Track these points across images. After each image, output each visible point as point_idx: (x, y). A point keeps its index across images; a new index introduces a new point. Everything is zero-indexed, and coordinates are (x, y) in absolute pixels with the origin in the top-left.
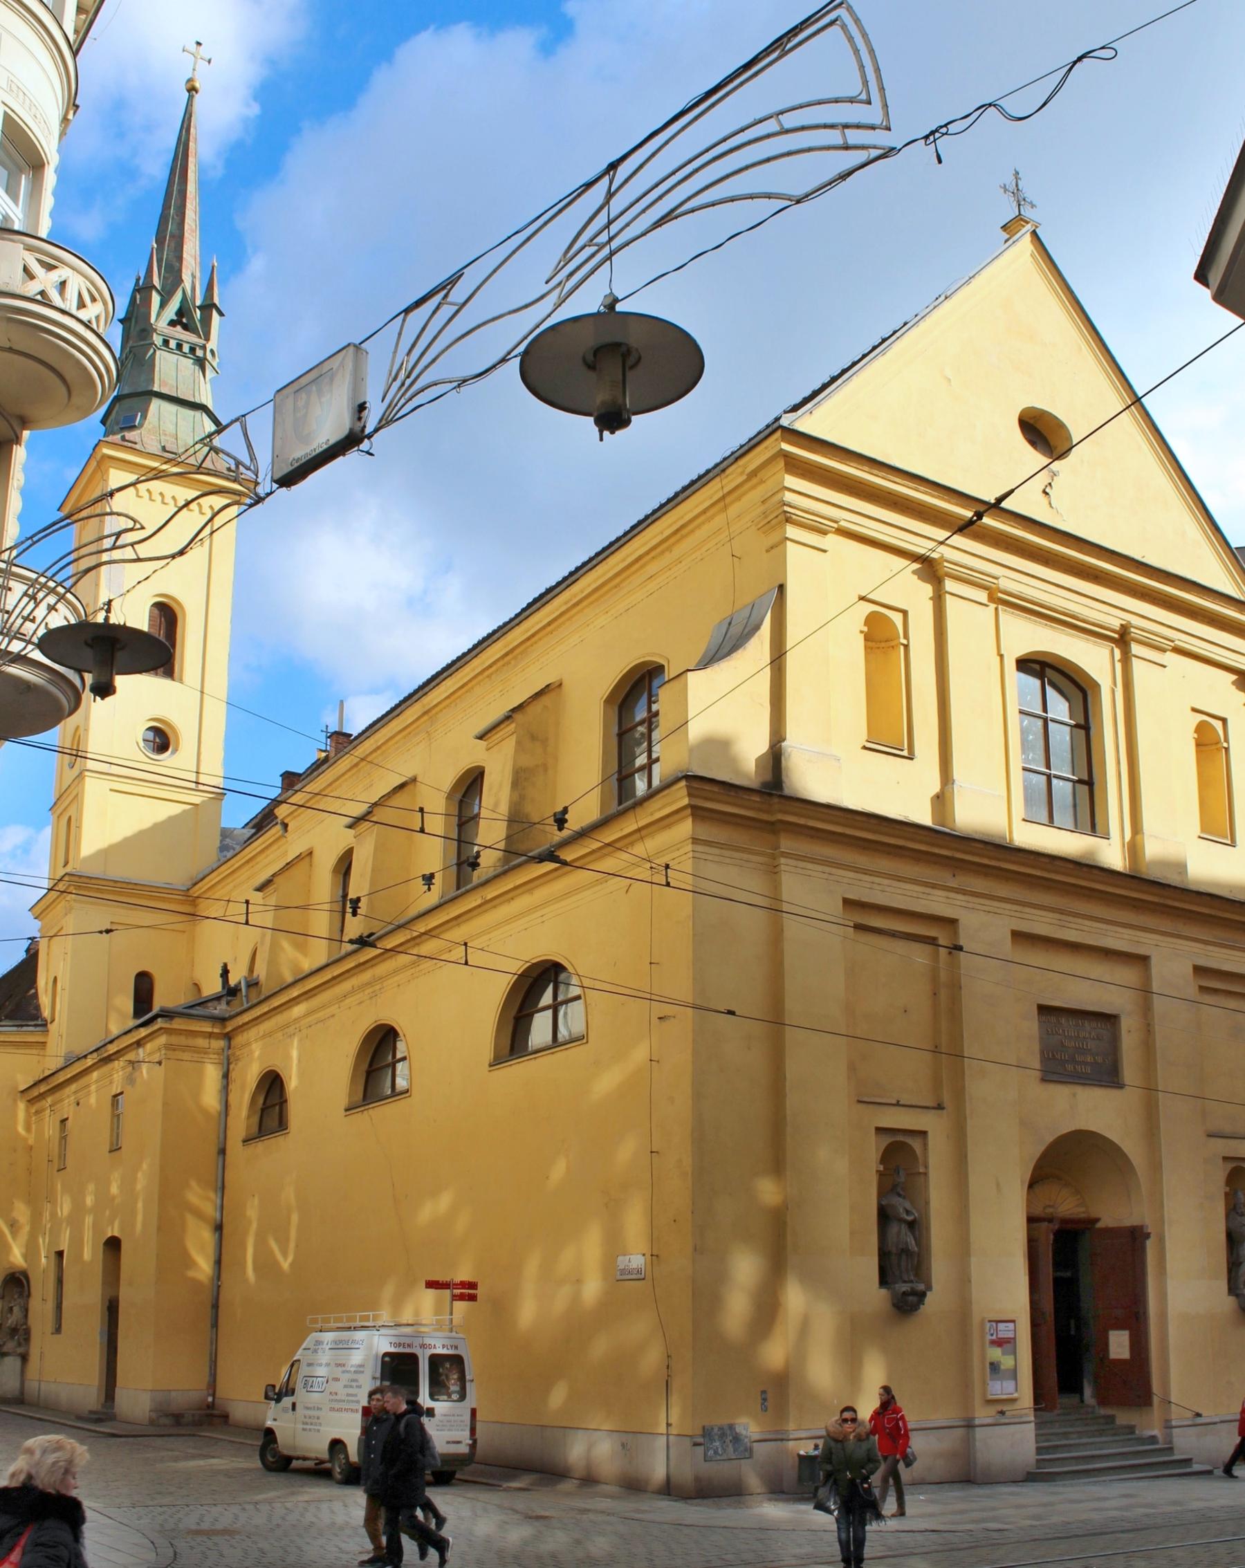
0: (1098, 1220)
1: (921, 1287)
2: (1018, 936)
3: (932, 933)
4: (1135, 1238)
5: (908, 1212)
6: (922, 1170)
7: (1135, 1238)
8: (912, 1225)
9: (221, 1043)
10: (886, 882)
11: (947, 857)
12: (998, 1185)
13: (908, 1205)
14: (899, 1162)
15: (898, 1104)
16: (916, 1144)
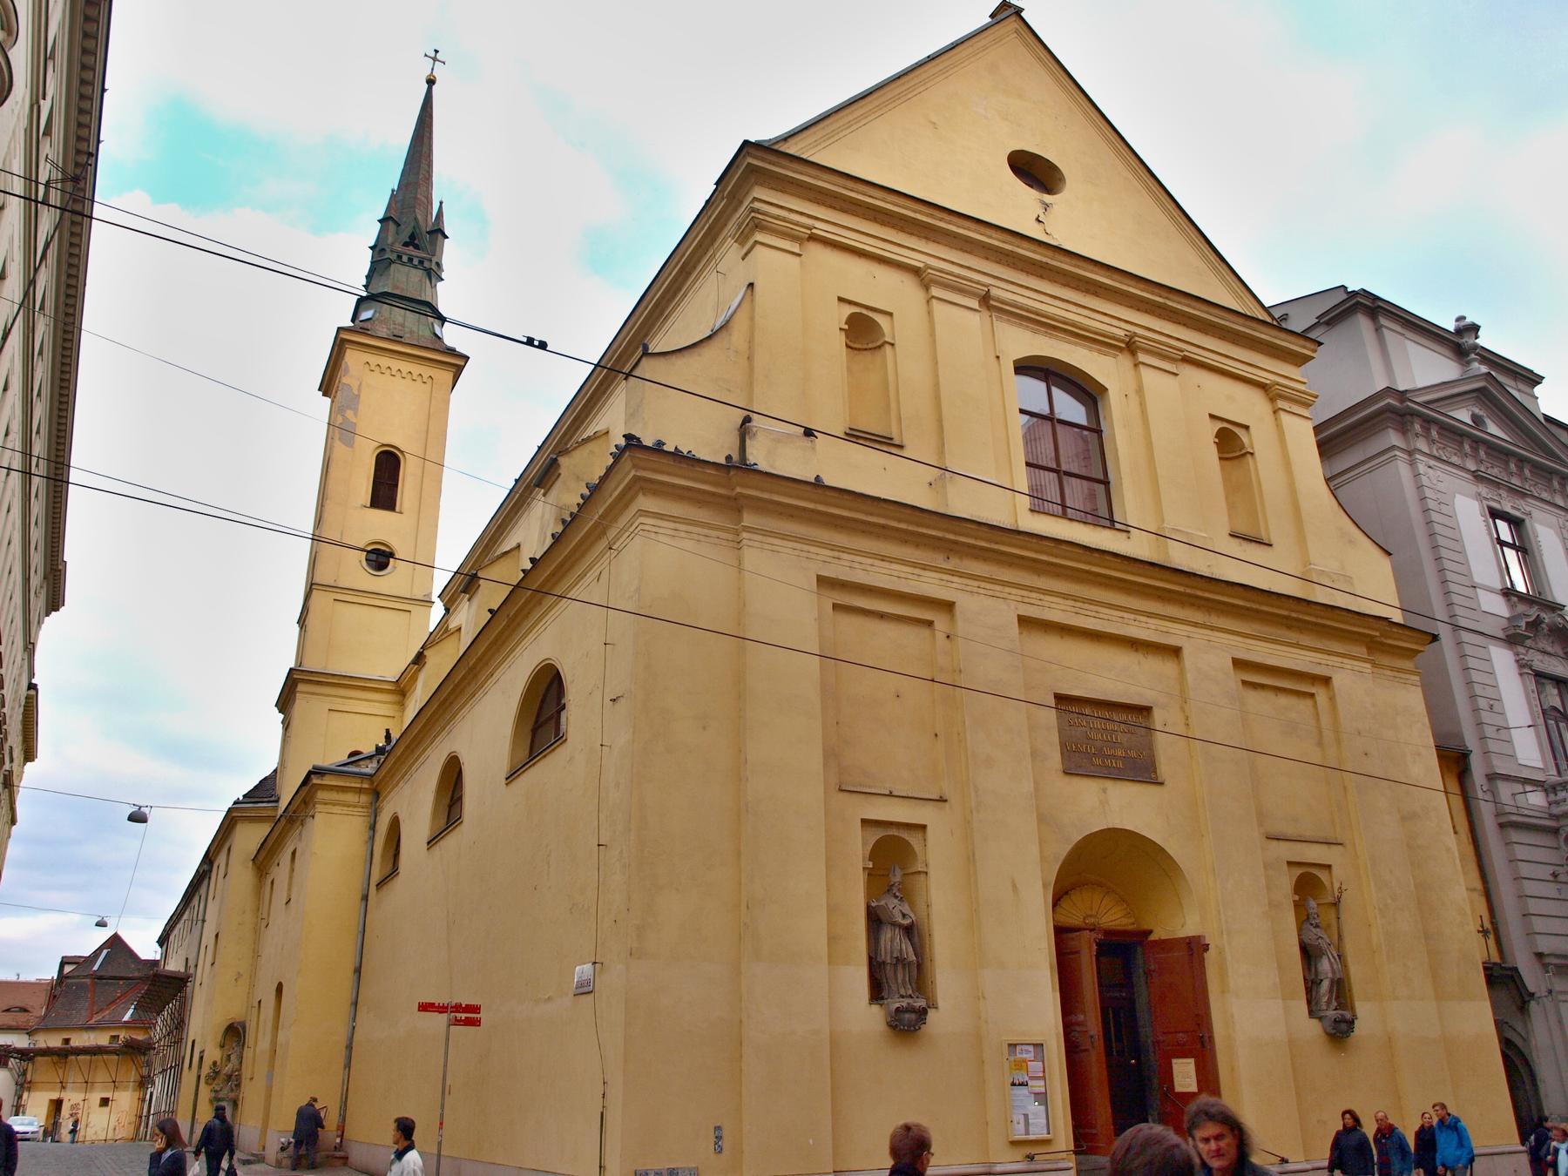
1: (921, 1003)
2: (1024, 621)
3: (926, 615)
4: (1195, 948)
5: (904, 916)
7: (1195, 948)
8: (909, 931)
10: (870, 561)
11: (939, 539)
12: (1014, 886)
13: (906, 909)
14: (891, 857)
15: (891, 795)
16: (913, 839)
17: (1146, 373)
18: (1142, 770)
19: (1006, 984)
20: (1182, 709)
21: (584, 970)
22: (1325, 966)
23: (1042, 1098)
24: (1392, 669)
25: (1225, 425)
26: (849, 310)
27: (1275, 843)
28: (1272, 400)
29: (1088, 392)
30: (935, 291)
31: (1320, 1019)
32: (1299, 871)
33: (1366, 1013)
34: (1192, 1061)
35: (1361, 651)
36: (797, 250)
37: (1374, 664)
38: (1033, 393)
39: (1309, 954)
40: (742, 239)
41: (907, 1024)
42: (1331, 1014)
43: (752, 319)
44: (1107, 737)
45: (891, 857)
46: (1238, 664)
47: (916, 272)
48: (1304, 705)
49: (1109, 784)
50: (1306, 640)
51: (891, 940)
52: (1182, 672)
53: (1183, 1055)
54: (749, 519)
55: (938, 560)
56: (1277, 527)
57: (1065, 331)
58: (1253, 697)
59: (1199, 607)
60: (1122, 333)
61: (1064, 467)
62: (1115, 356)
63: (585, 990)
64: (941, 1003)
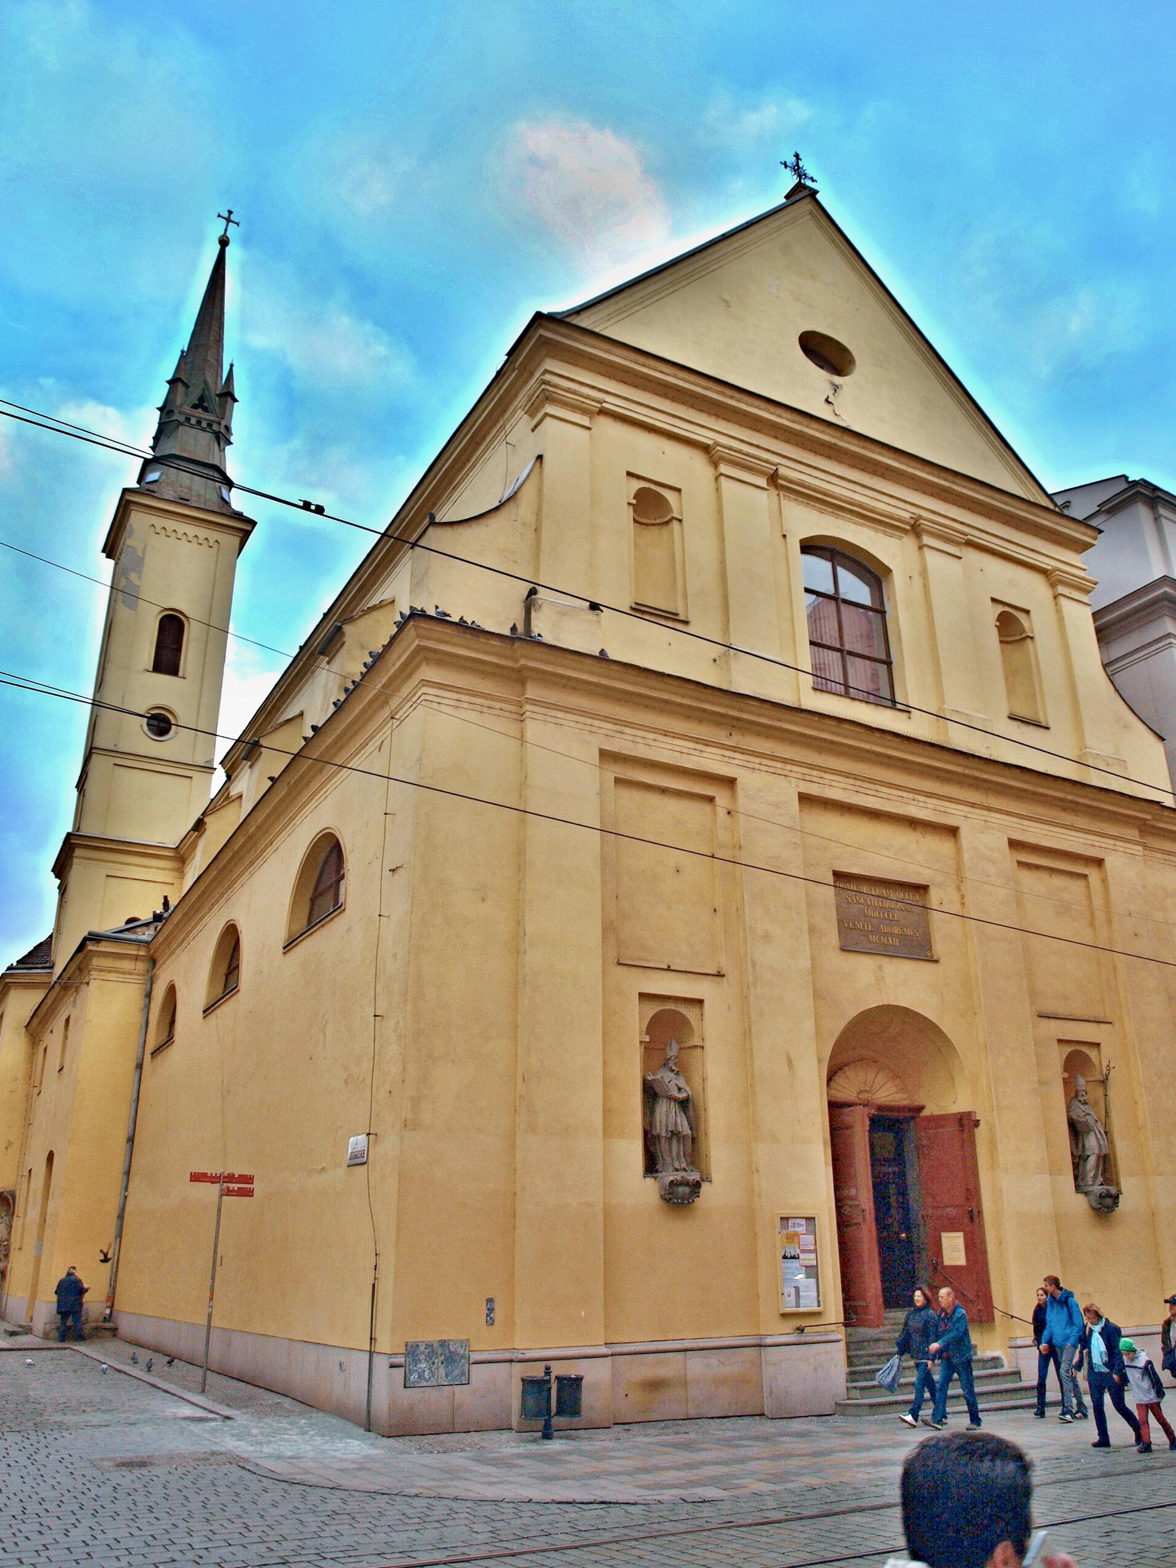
0: (922, 1108)
1: (694, 1176)
3: (708, 790)
4: (966, 1123)
5: (680, 1089)
6: (696, 1041)
7: (966, 1123)
9: (141, 966)
10: (652, 736)
12: (790, 1061)
13: (682, 1082)
14: (668, 1030)
15: (669, 969)
16: (690, 1013)
17: (931, 557)
18: (920, 949)
19: (780, 1160)
20: (959, 889)
21: (357, 1142)
22: (1092, 1143)
23: (812, 1271)
24: (1164, 852)
25: (1007, 609)
26: (637, 485)
27: (1046, 1020)
28: (1053, 585)
29: (874, 573)
30: (724, 468)
31: (1086, 1194)
32: (1068, 1049)
33: (1129, 1186)
34: (961, 1234)
35: (1133, 833)
36: (586, 422)
37: (1145, 846)
38: (818, 571)
39: (1076, 1130)
40: (531, 412)
41: (681, 1197)
42: (1097, 1189)
43: (540, 491)
44: (882, 914)
45: (668, 1030)
46: (1014, 844)
47: (705, 449)
48: (1077, 886)
49: (885, 961)
50: (1080, 822)
51: (666, 1113)
52: (959, 851)
53: (953, 1229)
54: (532, 691)
55: (721, 735)
56: (1054, 711)
57: (851, 512)
58: (1027, 877)
59: (977, 788)
60: (907, 515)
61: (848, 647)
62: (900, 538)
63: (358, 1161)
64: (714, 1176)
